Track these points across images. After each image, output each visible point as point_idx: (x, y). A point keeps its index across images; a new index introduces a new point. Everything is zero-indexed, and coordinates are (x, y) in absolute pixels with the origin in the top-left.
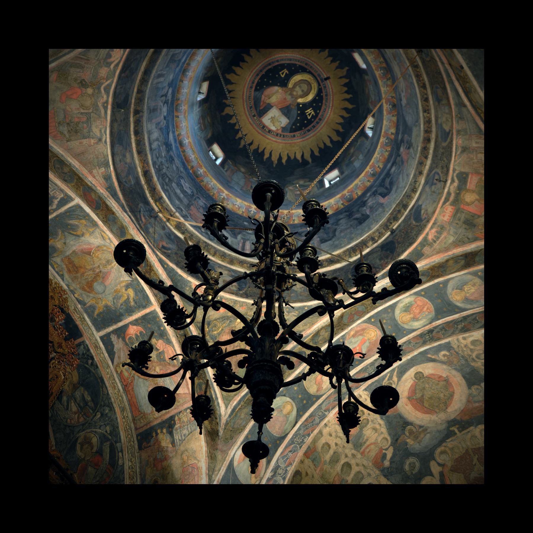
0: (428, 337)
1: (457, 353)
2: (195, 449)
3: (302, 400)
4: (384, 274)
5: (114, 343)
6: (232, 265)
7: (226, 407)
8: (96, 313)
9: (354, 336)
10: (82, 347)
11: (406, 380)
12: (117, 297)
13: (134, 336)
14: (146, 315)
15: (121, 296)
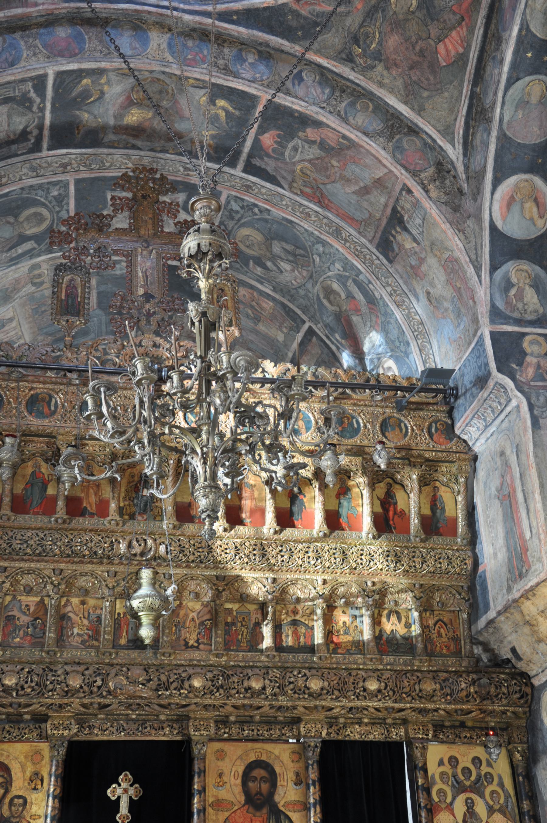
5: (263, 166)
7: (454, 146)
13: (275, 146)
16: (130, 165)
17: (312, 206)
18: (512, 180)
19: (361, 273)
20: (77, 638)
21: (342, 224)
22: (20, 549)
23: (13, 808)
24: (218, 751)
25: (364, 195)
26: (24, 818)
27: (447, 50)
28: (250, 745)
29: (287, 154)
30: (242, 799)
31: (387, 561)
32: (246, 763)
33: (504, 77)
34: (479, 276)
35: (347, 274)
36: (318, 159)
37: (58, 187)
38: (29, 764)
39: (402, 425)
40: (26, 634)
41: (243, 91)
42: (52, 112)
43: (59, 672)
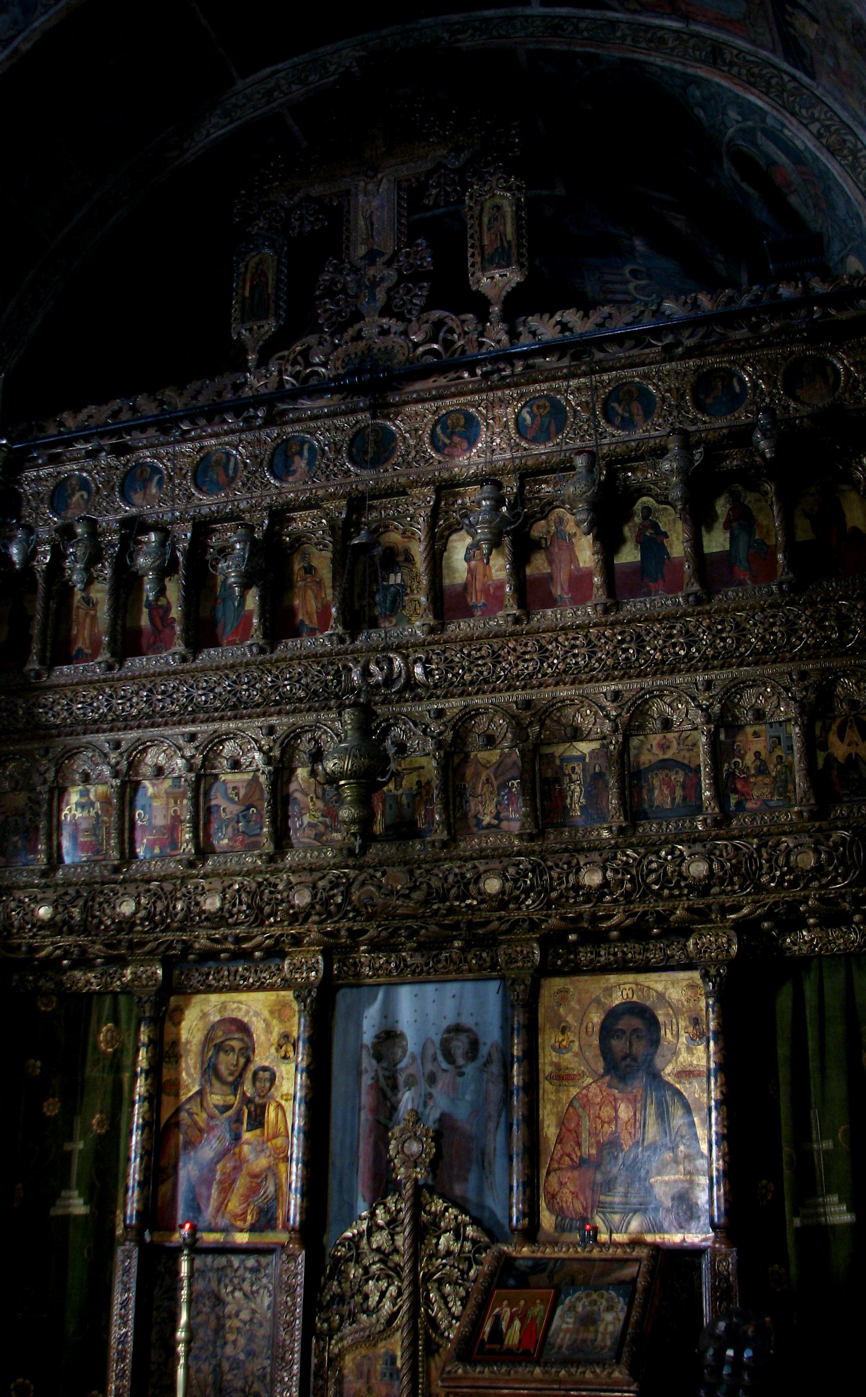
19: (767, 113)
20: (308, 832)
21: (723, 36)
22: (206, 702)
23: (258, 1084)
24: (560, 991)
26: (273, 1098)
28: (613, 978)
30: (600, 1066)
31: (824, 629)
32: (607, 1008)
35: (750, 123)
38: (275, 1022)
39: (829, 369)
40: (236, 831)
43: (280, 887)
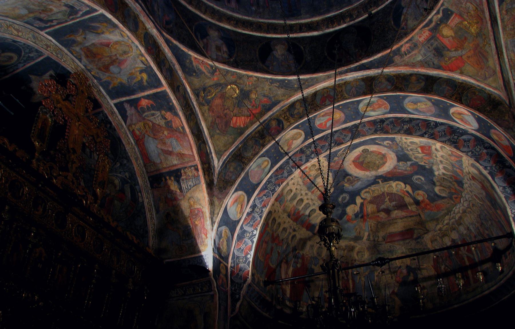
0: (379, 126)
1: (398, 144)
2: (199, 198)
3: (276, 157)
4: (356, 67)
5: (127, 109)
6: (220, 22)
7: (219, 161)
8: (111, 87)
9: (323, 116)
10: (101, 114)
11: (355, 152)
12: (131, 76)
13: (145, 107)
14: (157, 93)
15: (136, 77)
16: (73, 67)
17: (132, 139)
18: (240, 193)
19: (138, 185)
25: (167, 154)
27: (236, 122)
29: (146, 114)
33: (262, 152)
34: (213, 226)
35: (130, 181)
36: (159, 125)
37: (36, 54)
41: (159, 79)
42: (73, 23)
